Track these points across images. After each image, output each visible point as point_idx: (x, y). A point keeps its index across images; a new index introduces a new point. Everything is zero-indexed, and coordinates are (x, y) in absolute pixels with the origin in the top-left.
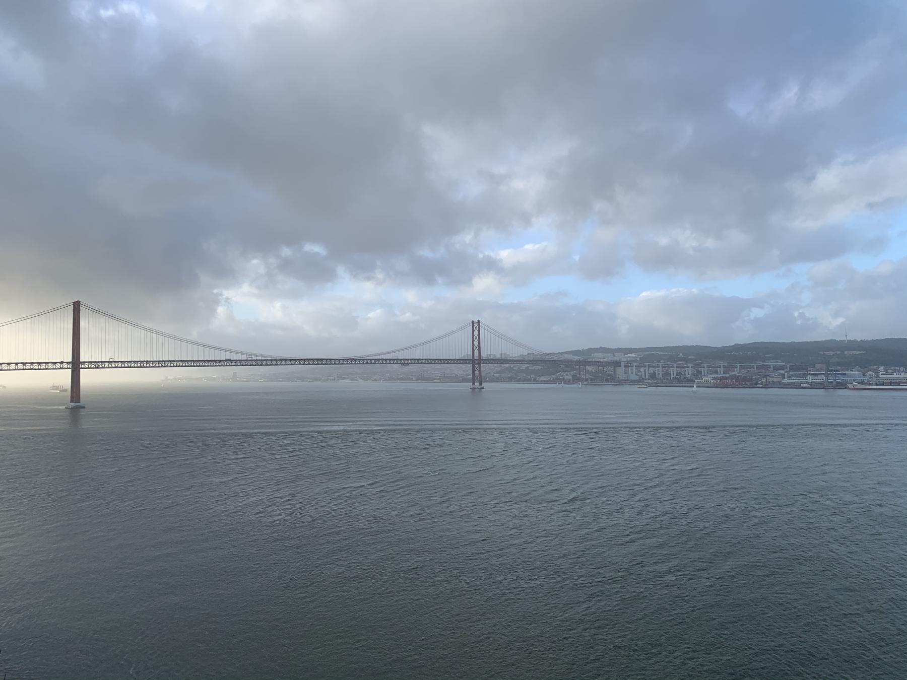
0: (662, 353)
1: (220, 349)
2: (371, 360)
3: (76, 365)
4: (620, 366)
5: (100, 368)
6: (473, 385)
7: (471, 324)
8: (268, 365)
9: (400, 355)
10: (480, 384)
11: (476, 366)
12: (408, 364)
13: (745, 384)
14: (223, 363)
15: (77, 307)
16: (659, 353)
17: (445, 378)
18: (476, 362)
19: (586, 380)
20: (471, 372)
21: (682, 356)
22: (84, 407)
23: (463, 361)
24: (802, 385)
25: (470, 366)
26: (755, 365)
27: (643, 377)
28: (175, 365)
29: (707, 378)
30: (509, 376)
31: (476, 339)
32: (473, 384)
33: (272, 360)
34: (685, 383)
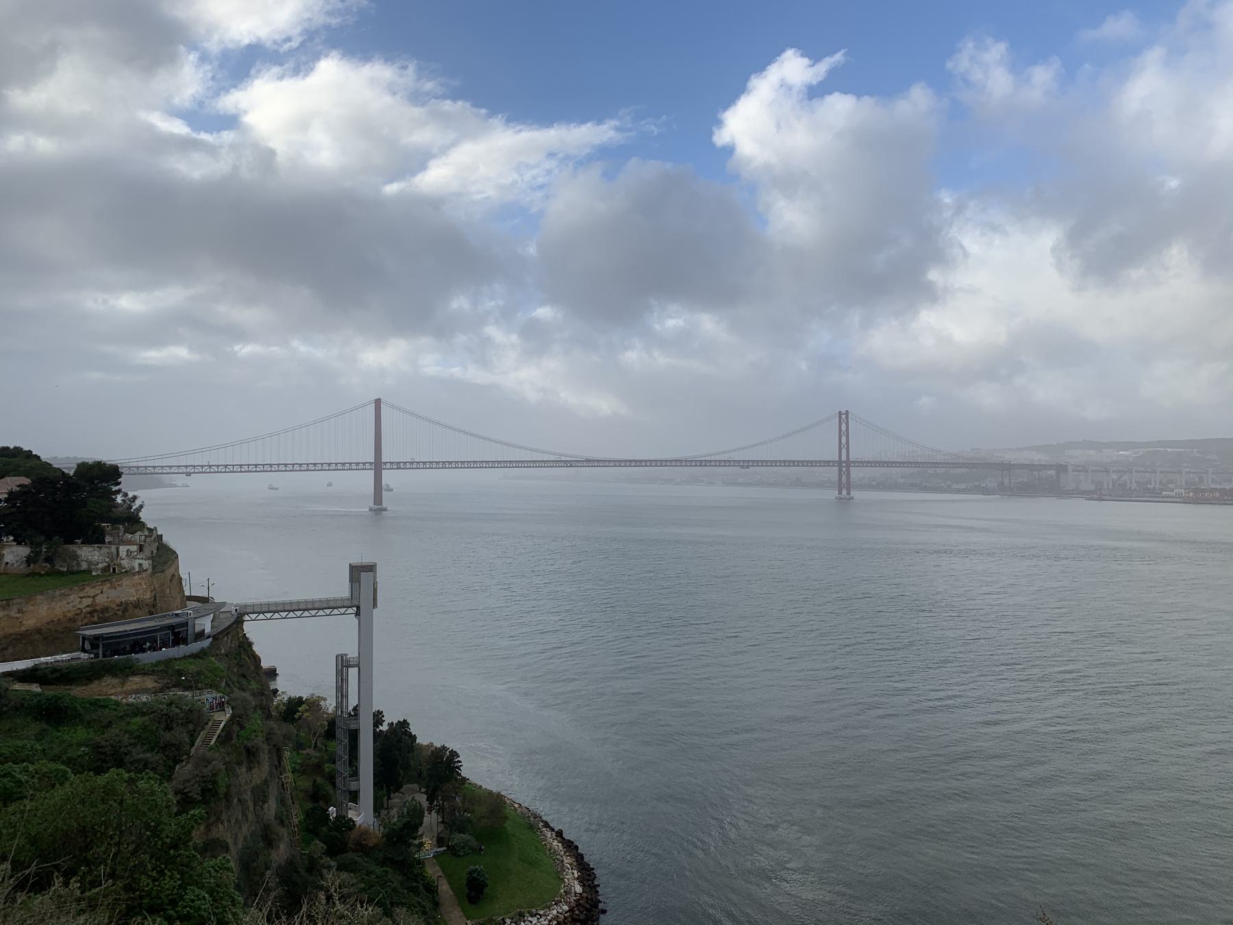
2: (701, 461)
3: (378, 466)
4: (1066, 471)
6: (839, 494)
10: (849, 493)
11: (844, 469)
12: (748, 467)
15: (378, 402)
16: (1169, 450)
18: (844, 465)
22: (385, 510)
23: (827, 463)
25: (837, 468)
28: (502, 465)
29: (1180, 490)
31: (844, 435)
32: (840, 493)
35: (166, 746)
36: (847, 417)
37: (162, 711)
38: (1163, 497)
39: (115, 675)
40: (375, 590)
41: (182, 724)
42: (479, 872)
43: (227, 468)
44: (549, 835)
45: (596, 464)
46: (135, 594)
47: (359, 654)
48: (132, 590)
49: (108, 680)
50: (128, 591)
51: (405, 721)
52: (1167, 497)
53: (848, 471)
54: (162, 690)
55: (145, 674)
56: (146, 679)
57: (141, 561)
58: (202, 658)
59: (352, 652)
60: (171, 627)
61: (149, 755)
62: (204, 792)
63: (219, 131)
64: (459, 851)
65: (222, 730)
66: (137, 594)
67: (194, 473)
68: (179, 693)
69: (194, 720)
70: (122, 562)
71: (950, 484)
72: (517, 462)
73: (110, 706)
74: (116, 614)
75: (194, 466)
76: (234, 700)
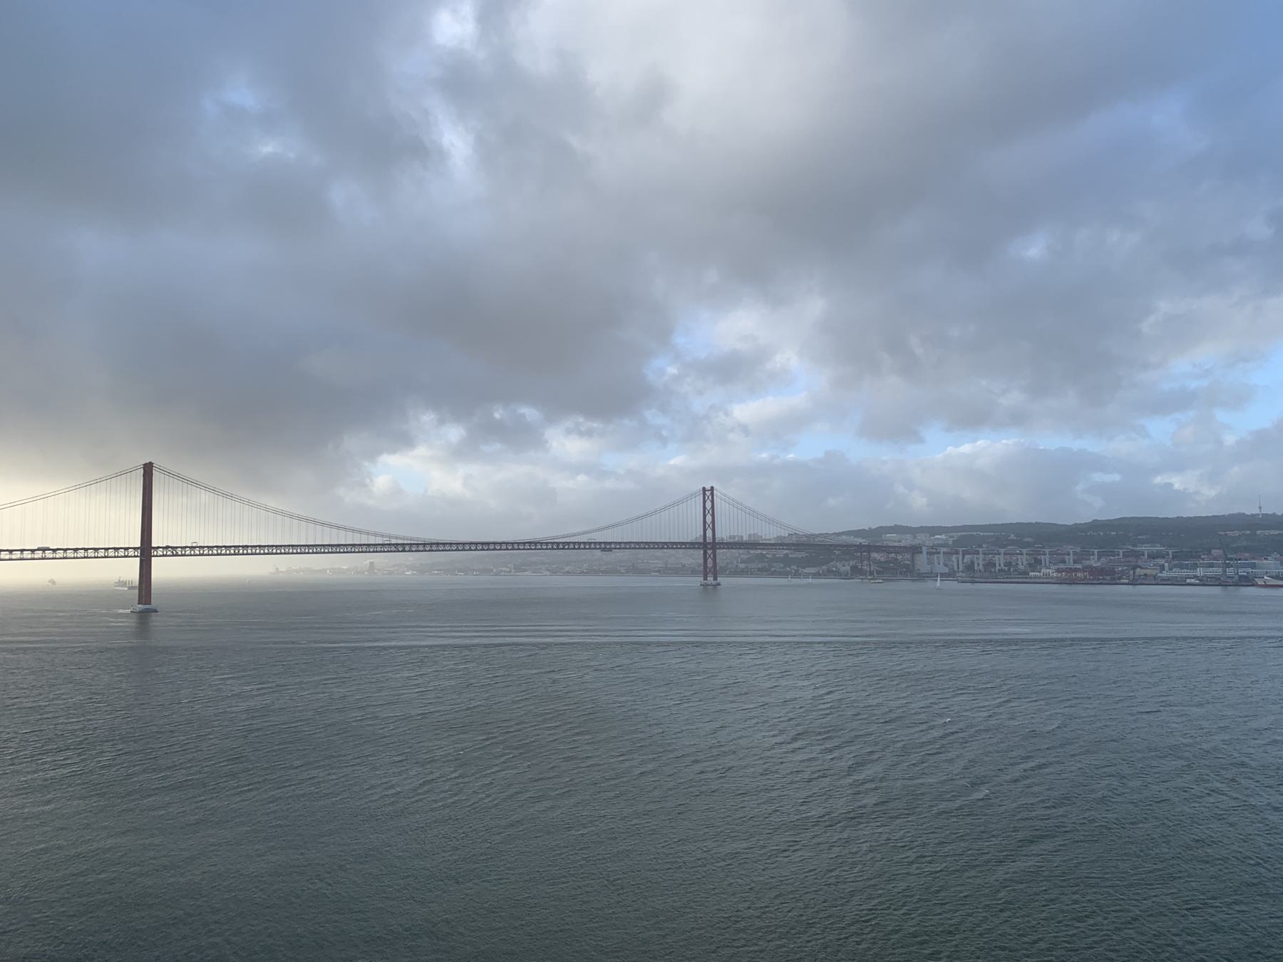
0: (985, 534)
1: (345, 529)
2: (558, 544)
3: (146, 552)
4: (921, 552)
5: (179, 556)
6: (704, 580)
7: (702, 492)
8: (412, 551)
9: (599, 537)
10: (715, 579)
11: (710, 552)
12: (610, 550)
13: (1103, 579)
14: (364, 549)
15: (148, 469)
17: (666, 571)
18: (709, 546)
19: (871, 573)
20: (701, 561)
21: (1015, 538)
22: (156, 611)
23: (692, 545)
24: (1188, 581)
26: (1121, 551)
27: (956, 569)
29: (1047, 570)
30: (760, 566)
32: (705, 579)
33: (417, 544)
34: (1015, 578)
36: (712, 494)
38: (1031, 578)
52: (1035, 578)
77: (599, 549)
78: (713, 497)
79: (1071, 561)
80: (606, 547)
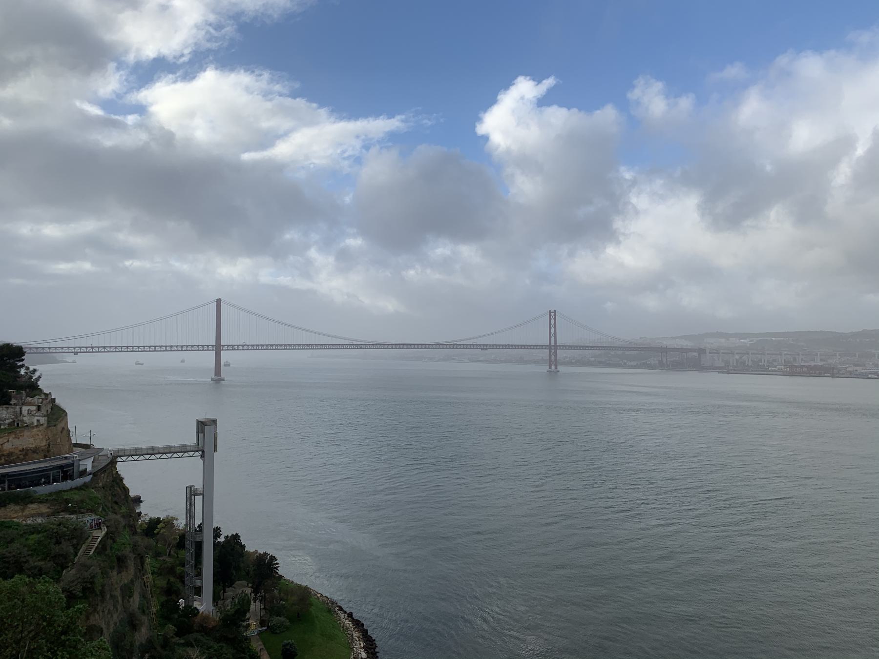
3: (218, 348)
4: (705, 353)
6: (549, 368)
7: (549, 314)
10: (556, 368)
11: (553, 351)
12: (486, 349)
15: (219, 301)
16: (774, 339)
18: (553, 348)
23: (542, 347)
24: (870, 376)
25: (548, 350)
29: (781, 367)
31: (553, 326)
32: (550, 367)
35: (55, 556)
36: (555, 315)
37: (53, 530)
38: (770, 371)
39: (17, 503)
40: (216, 439)
41: (69, 540)
42: (291, 645)
43: (105, 349)
44: (342, 616)
45: (379, 347)
46: (33, 442)
47: (203, 486)
48: (32, 440)
49: (12, 507)
50: (27, 440)
51: (237, 534)
52: (773, 371)
53: (556, 352)
54: (53, 514)
55: (41, 502)
56: (41, 506)
57: (38, 418)
58: (84, 490)
59: (199, 485)
60: (61, 467)
61: (42, 563)
62: (84, 589)
63: (125, 115)
64: (276, 629)
65: (99, 544)
66: (35, 442)
67: (80, 352)
68: (66, 516)
69: (78, 536)
70: (24, 418)
71: (626, 361)
72: (321, 345)
73: (13, 527)
74: (18, 457)
75: (80, 348)
76: (110, 520)
77: (480, 348)
78: (555, 317)
79: (819, 360)
80: (485, 347)
